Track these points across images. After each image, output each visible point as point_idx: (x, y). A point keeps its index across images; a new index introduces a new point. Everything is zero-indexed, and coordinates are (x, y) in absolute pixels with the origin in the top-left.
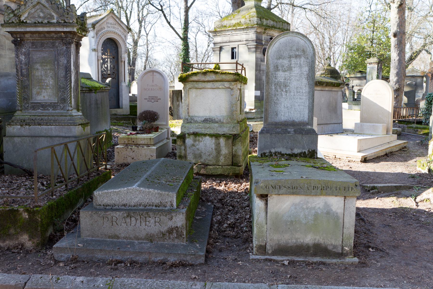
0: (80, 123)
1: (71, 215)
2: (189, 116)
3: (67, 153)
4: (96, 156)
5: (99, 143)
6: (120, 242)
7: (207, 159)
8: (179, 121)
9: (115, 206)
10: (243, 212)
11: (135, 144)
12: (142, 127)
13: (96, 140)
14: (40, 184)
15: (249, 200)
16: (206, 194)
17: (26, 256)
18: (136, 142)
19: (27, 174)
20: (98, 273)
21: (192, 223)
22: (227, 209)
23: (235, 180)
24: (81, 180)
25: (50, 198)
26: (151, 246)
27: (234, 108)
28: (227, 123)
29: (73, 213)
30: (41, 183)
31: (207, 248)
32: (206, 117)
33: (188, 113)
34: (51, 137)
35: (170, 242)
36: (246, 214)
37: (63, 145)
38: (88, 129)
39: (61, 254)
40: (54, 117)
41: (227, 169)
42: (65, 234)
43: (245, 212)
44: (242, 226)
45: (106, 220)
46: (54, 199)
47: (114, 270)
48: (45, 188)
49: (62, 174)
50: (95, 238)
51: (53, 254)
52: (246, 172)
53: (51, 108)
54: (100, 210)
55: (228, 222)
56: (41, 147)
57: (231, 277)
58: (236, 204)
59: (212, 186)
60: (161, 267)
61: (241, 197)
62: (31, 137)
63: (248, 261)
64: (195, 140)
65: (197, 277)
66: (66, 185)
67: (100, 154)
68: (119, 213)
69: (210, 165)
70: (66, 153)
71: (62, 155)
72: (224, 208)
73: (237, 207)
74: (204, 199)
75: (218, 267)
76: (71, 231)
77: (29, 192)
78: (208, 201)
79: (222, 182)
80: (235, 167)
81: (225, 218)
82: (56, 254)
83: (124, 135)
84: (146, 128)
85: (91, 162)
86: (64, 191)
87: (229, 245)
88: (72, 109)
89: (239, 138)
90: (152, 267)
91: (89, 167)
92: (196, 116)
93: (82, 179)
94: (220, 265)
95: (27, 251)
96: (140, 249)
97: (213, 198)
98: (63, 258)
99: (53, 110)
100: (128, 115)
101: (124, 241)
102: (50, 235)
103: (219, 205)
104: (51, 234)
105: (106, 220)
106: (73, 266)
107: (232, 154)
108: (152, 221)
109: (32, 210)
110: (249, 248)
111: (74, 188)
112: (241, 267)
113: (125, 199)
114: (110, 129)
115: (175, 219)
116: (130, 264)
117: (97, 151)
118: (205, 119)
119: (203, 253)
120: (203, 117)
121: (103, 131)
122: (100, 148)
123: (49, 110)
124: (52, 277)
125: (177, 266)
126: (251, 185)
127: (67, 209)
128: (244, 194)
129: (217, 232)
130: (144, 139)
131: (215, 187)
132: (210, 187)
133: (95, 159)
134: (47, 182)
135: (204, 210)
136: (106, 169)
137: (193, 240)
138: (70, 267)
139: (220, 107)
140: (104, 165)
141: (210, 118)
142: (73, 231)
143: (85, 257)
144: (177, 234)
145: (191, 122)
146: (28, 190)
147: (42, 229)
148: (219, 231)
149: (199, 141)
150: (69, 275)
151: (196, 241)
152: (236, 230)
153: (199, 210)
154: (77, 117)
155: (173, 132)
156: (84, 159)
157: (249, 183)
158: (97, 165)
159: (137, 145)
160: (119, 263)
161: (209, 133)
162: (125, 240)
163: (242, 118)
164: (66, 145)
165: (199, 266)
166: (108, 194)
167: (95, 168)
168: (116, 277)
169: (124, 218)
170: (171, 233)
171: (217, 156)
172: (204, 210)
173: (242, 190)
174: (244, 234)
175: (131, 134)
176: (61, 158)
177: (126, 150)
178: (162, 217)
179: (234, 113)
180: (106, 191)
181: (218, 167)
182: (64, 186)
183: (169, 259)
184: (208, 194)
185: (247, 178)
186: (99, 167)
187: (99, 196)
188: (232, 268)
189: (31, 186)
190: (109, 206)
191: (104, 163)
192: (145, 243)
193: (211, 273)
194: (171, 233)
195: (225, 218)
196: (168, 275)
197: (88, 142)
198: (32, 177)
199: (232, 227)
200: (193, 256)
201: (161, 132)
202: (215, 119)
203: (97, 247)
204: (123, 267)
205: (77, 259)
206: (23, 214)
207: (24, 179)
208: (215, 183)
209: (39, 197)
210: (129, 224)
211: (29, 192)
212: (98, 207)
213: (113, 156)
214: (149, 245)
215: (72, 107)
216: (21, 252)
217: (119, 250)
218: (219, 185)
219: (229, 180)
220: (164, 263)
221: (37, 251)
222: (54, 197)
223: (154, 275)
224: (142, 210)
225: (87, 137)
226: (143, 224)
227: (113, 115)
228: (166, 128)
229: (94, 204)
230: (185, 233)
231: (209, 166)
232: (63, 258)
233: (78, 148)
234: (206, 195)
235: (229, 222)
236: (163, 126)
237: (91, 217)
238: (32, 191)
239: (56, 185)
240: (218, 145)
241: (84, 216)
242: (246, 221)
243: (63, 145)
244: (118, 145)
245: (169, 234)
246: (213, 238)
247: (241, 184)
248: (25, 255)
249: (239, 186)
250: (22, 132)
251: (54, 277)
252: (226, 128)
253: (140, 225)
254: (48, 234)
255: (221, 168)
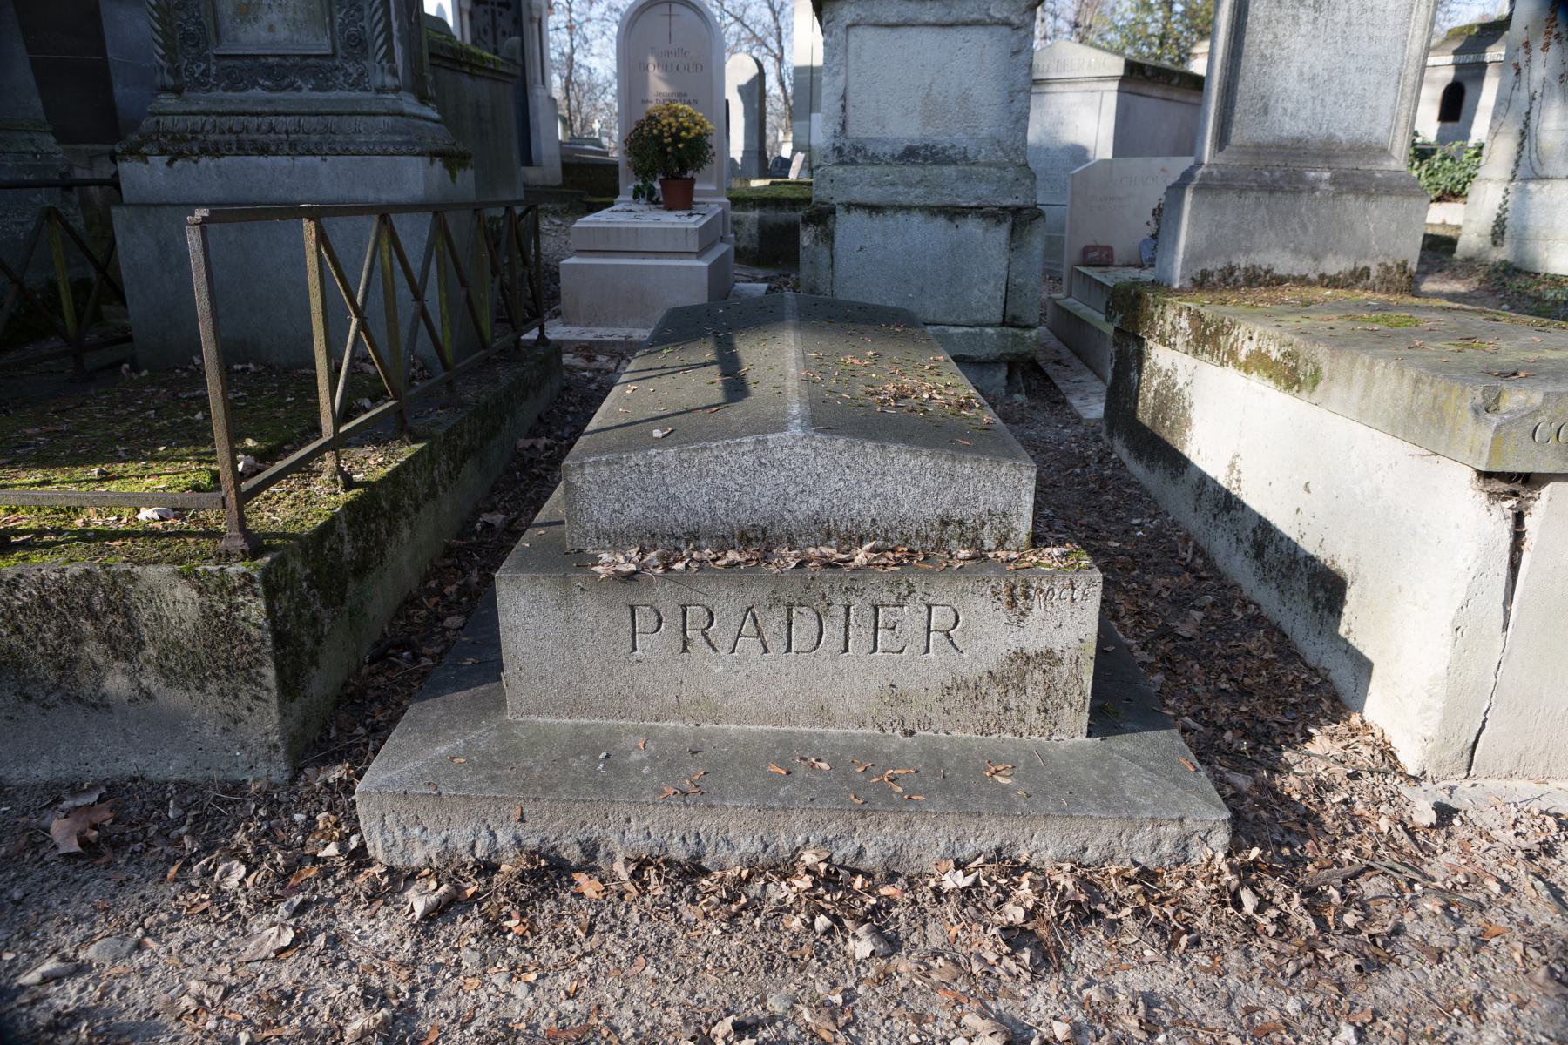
32: (913, 141)
154: (422, 122)
215: (395, 74)
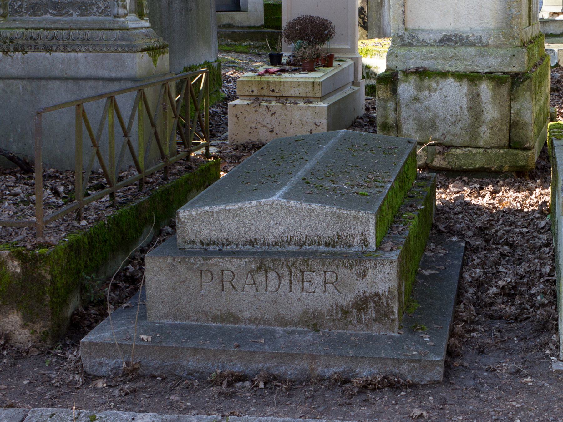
0: (145, 46)
1: (123, 266)
2: (406, 30)
3: (113, 117)
4: (184, 126)
5: (189, 95)
6: (241, 331)
7: (448, 132)
8: (381, 41)
9: (230, 243)
10: (535, 258)
11: (276, 97)
12: (294, 57)
13: (184, 87)
14: (48, 191)
15: (549, 230)
16: (446, 215)
17: (15, 365)
18: (280, 91)
19: (19, 168)
20: (189, 404)
21: (413, 284)
22: (496, 252)
23: (515, 181)
24: (147, 183)
25: (74, 226)
26: (314, 340)
27: (514, 10)
28: (497, 46)
29: (129, 262)
30: (52, 189)
31: (448, 345)
32: (448, 31)
33: (404, 22)
34: (75, 79)
35: (361, 330)
36: (543, 265)
37: (104, 100)
38: (164, 60)
39: (99, 360)
40: (81, 32)
41: (497, 155)
42: (109, 312)
43: (540, 258)
44: (533, 292)
45: (206, 278)
46: (83, 228)
47: (226, 398)
48: (61, 201)
49: (103, 167)
50: (180, 320)
51: (80, 358)
52: (543, 163)
53: (75, 11)
54: (193, 253)
55: (500, 282)
56: (51, 104)
57: (506, 415)
58: (519, 240)
59: (462, 197)
60: (338, 390)
61: (529, 224)
62: (28, 79)
63: (549, 375)
64: (420, 87)
65: (425, 414)
66: (112, 195)
67: (193, 121)
68: (239, 260)
69: (456, 147)
70: (111, 118)
71: (102, 124)
72: (490, 250)
73: (521, 246)
74: (442, 227)
75: (474, 389)
76: (124, 305)
77: (22, 210)
78: (452, 232)
79: (486, 188)
80: (516, 151)
81: (493, 274)
82: (87, 360)
83: (250, 74)
84: (303, 59)
85: (170, 140)
86: (107, 207)
87: (502, 337)
88: (126, 12)
89: (526, 83)
90: (318, 390)
91: (167, 152)
92: (422, 30)
93: (151, 180)
94: (479, 386)
95: (18, 351)
96: (288, 347)
97: (463, 224)
98: (104, 369)
99: (80, 15)
100: (260, 27)
101: (250, 329)
102: (73, 314)
103: (478, 242)
104: (76, 313)
105: (206, 278)
106: (128, 389)
107: (508, 120)
108: (318, 280)
109: (30, 254)
110: (551, 345)
111: (131, 201)
112: (531, 391)
113: (253, 228)
114: (217, 60)
115: (372, 276)
116: (265, 383)
117: (186, 113)
118: (445, 36)
119: (439, 358)
120: (439, 31)
121: (200, 65)
122: (193, 106)
123: (72, 15)
124: (79, 414)
125: (378, 388)
126: (554, 195)
127: (113, 251)
128: (538, 215)
129: (472, 307)
130: (299, 84)
131: (468, 199)
132: (456, 199)
133: (180, 133)
134: (66, 186)
135: (442, 253)
136: (207, 155)
137: (415, 327)
138: (121, 390)
139: (480, 7)
140: (203, 146)
141: (456, 35)
142: (128, 304)
143: (157, 366)
144: (377, 312)
145: (410, 45)
146: (22, 206)
147: (54, 300)
148: (478, 304)
149: (429, 88)
150: (119, 409)
151: (422, 329)
152: (517, 301)
153: (429, 254)
154: (138, 31)
155: (368, 67)
156: (156, 133)
157: (550, 189)
158: (185, 147)
159: (282, 99)
160: (239, 381)
161: (453, 69)
162: (253, 327)
163: (534, 35)
164: (111, 98)
165: (430, 388)
166: (213, 215)
167: (182, 154)
168: (232, 414)
169: (250, 272)
170: (363, 309)
171: (472, 125)
172: (442, 253)
173: (532, 206)
174: (539, 312)
175: (267, 71)
176: (100, 130)
177: (256, 111)
178: (341, 271)
179: (514, 22)
180: (207, 208)
181: (475, 151)
182: (107, 198)
183: (358, 370)
184: (452, 216)
185: (546, 178)
186: (190, 152)
187: (190, 221)
188: (510, 392)
189: (28, 198)
190: (214, 243)
191: (202, 142)
192: (300, 333)
193: (460, 404)
194: (363, 309)
195: (493, 274)
196: (356, 409)
197: (165, 92)
198: (30, 175)
199: (509, 295)
200: (417, 365)
201: (340, 69)
202: (468, 37)
203: (186, 342)
204: (248, 391)
205: (139, 371)
206: (10, 263)
207: (11, 180)
208: (467, 190)
209: (47, 222)
210: (262, 287)
211: (22, 210)
212: (188, 247)
213: (223, 126)
214: (309, 337)
215: (125, 7)
216: (3, 355)
217: (238, 349)
218: (479, 193)
219: (501, 183)
220: (347, 381)
221: (43, 352)
222: (84, 222)
223: (322, 408)
224: (294, 254)
225: (163, 78)
226: (297, 287)
227: (224, 26)
228: (351, 59)
229: (180, 240)
230: (396, 310)
231: (453, 150)
232: (104, 369)
233: (141, 106)
234: (446, 218)
235: (501, 283)
236: (343, 53)
237: (170, 270)
238: (31, 208)
239: (89, 195)
240: (475, 98)
241: (155, 268)
242: (542, 280)
243: (104, 100)
244: (235, 97)
245: (359, 310)
246: (464, 321)
247: (531, 191)
248: (12, 361)
249: (527, 197)
250: (7, 67)
251: (82, 415)
252: (496, 57)
253: (288, 289)
254: (69, 311)
255: (484, 154)
